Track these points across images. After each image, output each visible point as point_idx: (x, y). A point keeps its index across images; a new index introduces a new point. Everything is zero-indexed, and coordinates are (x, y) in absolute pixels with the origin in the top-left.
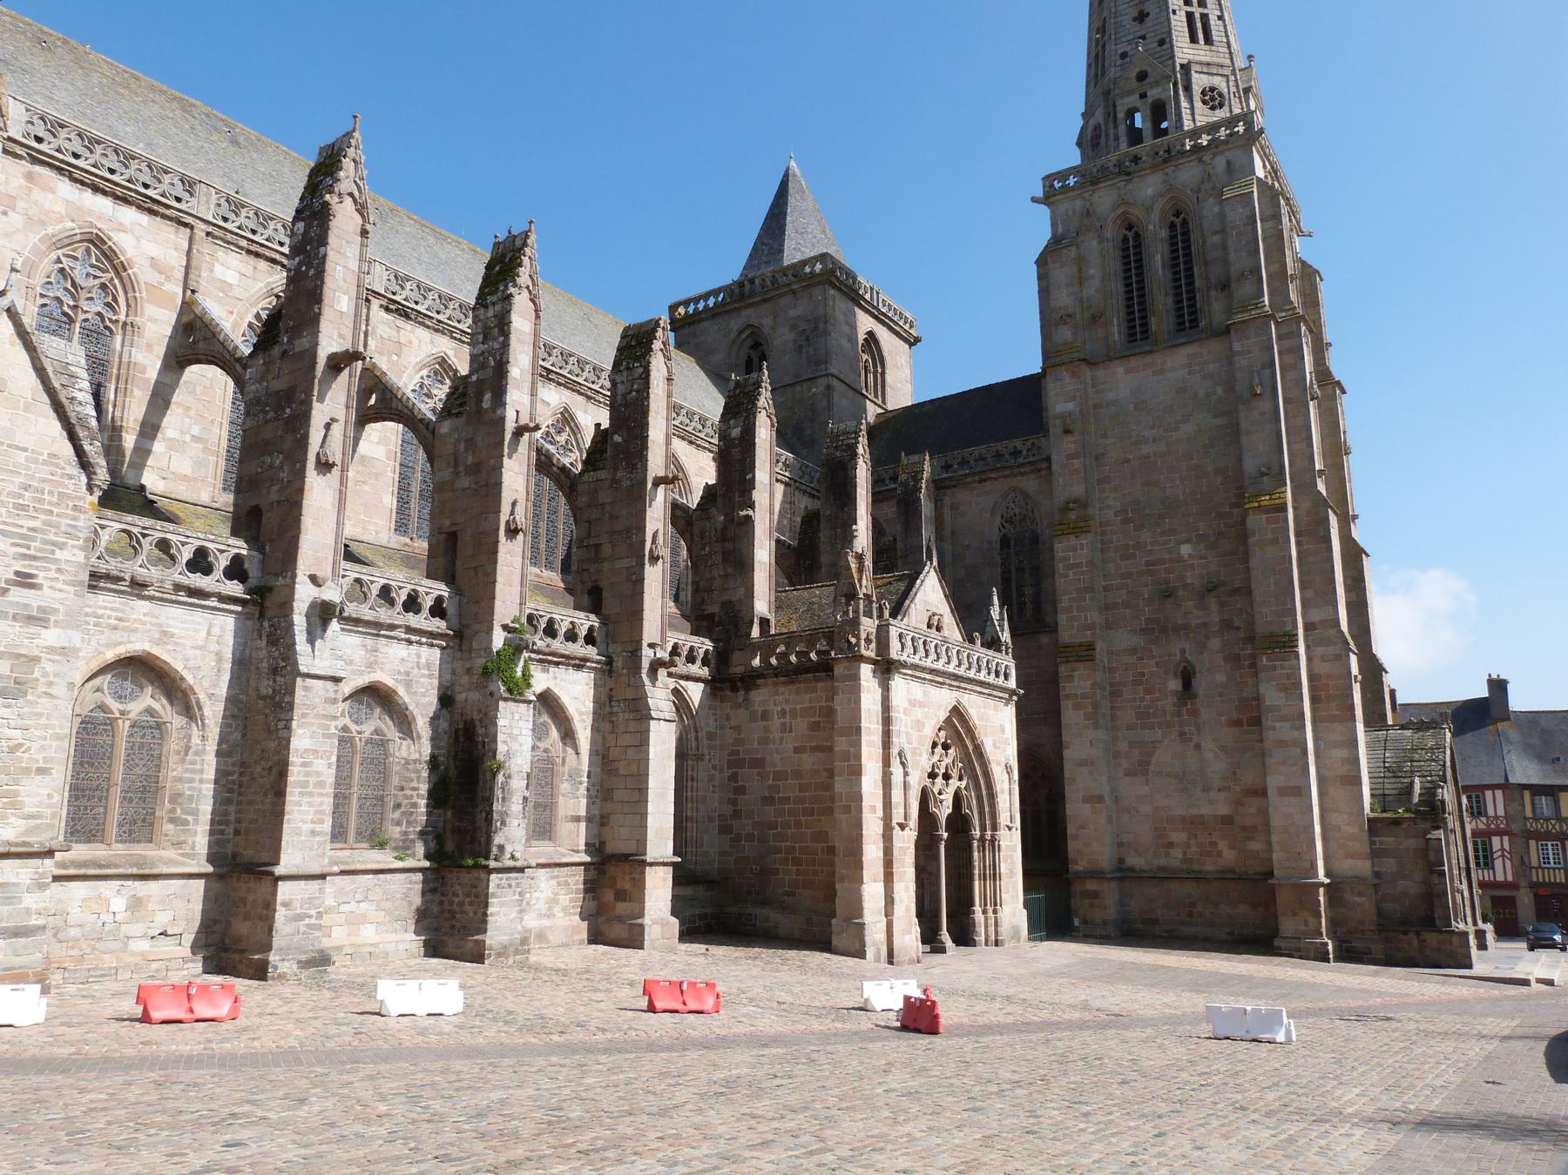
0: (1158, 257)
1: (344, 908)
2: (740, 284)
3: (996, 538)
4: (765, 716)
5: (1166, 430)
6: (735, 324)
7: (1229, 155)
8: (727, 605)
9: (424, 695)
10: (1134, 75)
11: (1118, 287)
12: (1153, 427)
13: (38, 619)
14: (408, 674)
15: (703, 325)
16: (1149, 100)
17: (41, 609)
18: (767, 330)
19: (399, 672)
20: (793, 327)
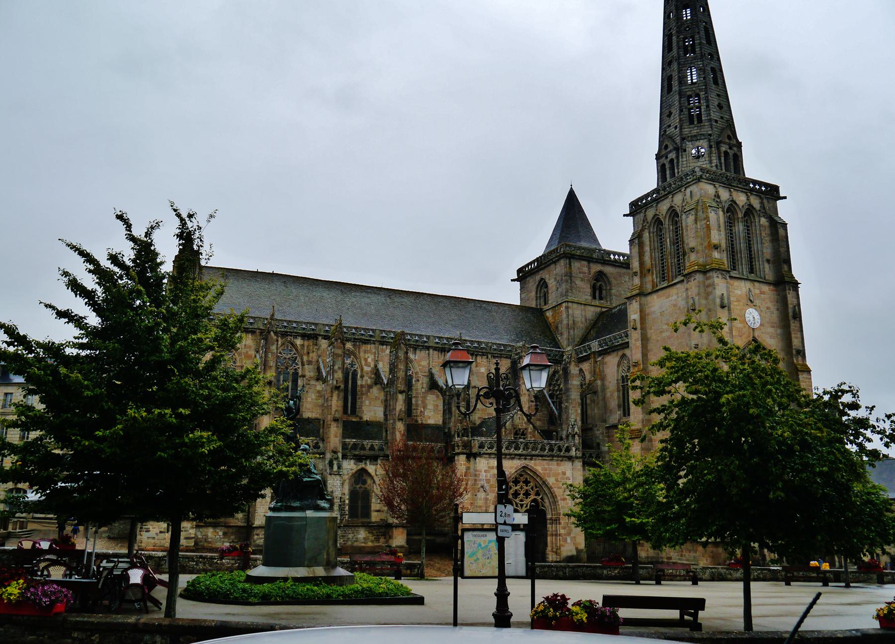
0: (668, 240)
3: (620, 378)
10: (663, 147)
11: (657, 255)
15: (528, 279)
16: (669, 159)
18: (547, 281)
20: (555, 279)
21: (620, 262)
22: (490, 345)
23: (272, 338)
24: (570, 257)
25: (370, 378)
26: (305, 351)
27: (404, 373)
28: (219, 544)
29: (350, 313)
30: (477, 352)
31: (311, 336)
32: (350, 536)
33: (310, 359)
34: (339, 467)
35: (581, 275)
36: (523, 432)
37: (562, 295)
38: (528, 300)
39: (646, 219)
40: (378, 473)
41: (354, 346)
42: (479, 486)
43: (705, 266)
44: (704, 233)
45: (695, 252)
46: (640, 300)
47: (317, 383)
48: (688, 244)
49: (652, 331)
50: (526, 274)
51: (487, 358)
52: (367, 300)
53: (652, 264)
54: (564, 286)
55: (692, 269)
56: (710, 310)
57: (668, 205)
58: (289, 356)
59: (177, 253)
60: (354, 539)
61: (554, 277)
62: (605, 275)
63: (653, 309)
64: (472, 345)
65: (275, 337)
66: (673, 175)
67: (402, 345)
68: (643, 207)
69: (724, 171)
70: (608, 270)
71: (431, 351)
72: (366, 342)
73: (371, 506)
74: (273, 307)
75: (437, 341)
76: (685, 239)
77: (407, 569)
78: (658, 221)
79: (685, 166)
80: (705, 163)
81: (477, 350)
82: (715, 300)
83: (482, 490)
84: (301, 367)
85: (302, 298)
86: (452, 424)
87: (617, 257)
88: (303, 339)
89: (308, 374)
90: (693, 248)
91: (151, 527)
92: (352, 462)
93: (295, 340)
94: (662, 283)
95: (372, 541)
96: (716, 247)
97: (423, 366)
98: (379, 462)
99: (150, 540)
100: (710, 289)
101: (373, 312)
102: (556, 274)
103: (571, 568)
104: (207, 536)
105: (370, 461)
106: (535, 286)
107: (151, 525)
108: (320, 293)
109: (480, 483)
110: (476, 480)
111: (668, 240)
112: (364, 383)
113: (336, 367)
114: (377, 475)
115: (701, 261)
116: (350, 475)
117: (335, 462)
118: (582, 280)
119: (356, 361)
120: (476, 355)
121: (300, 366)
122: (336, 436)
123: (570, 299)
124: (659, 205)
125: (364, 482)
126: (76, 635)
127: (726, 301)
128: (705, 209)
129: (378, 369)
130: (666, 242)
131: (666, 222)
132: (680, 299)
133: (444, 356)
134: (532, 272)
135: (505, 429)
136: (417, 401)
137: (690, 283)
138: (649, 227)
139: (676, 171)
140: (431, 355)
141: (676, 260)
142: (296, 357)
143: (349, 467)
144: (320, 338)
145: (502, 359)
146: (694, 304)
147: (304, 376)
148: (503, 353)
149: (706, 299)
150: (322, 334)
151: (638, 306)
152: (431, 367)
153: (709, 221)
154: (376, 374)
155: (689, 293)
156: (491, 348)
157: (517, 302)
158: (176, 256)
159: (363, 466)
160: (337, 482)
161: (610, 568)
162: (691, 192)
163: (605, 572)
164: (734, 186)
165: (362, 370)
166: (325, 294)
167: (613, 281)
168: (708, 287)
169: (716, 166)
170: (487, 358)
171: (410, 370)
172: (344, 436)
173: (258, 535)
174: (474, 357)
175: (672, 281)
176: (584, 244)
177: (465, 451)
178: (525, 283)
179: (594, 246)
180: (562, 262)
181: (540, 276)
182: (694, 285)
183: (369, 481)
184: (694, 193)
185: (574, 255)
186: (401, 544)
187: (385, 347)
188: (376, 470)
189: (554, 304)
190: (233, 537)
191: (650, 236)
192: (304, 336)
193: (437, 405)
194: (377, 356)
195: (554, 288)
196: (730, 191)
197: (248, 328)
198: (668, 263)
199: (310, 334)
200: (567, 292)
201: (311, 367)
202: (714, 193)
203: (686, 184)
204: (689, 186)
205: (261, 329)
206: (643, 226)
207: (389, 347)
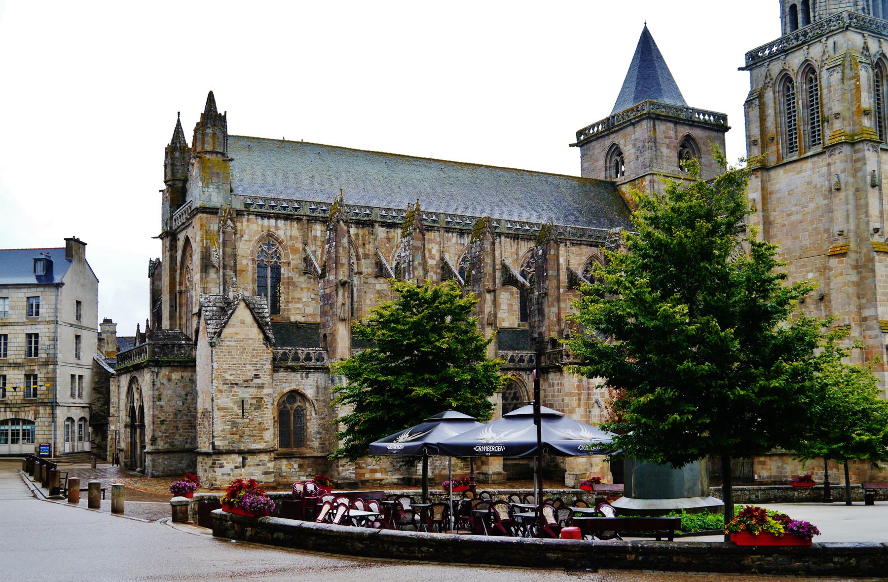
0: (800, 102)
1: (369, 467)
2: (608, 119)
4: (553, 386)
5: (802, 207)
6: (608, 142)
7: (835, 38)
8: (540, 334)
11: (784, 120)
12: (796, 205)
13: (261, 387)
15: (593, 143)
17: (262, 384)
18: (621, 147)
20: (634, 145)
21: (711, 124)
23: (342, 229)
24: (656, 118)
25: (436, 273)
26: (360, 241)
27: (491, 269)
28: (295, 478)
29: (403, 193)
31: (366, 223)
32: (438, 463)
33: (367, 252)
35: (667, 141)
37: (644, 166)
38: (594, 170)
39: (770, 75)
42: (594, 401)
43: (852, 136)
44: (852, 95)
45: (841, 119)
46: (762, 175)
47: (376, 281)
48: (830, 109)
49: (776, 213)
50: (591, 137)
51: (566, 245)
53: (777, 132)
54: (647, 155)
55: (837, 139)
56: (857, 190)
57: (802, 59)
59: (199, 120)
60: (442, 467)
61: (633, 142)
62: (693, 140)
63: (777, 187)
64: (531, 228)
65: (345, 228)
66: (807, 21)
68: (765, 60)
69: (872, 15)
70: (697, 133)
71: (503, 238)
75: (509, 226)
76: (825, 101)
78: (786, 78)
79: (824, 8)
80: (848, 5)
82: (865, 177)
83: (596, 405)
84: (356, 262)
85: (344, 174)
86: (544, 328)
87: (707, 117)
88: (357, 227)
89: (365, 270)
90: (839, 114)
91: (225, 462)
94: (790, 155)
95: (461, 468)
96: (866, 113)
99: (226, 477)
100: (859, 165)
102: (636, 140)
103: (763, 490)
106: (604, 153)
107: (225, 460)
108: (362, 166)
109: (594, 398)
110: (589, 394)
111: (800, 102)
113: (416, 263)
115: (848, 130)
118: (668, 147)
123: (654, 170)
124: (788, 58)
126: (836, 559)
127: (877, 181)
128: (854, 65)
129: (446, 262)
130: (798, 104)
131: (798, 81)
132: (816, 175)
133: (518, 244)
134: (598, 136)
137: (833, 157)
138: (774, 85)
139: (812, 14)
140: (503, 244)
141: (809, 126)
144: (377, 225)
145: (582, 246)
146: (838, 183)
147: (360, 273)
148: (584, 239)
149: (855, 176)
150: (379, 220)
151: (760, 183)
152: (503, 258)
153: (858, 80)
154: (443, 268)
155: (833, 169)
157: (578, 174)
158: (198, 124)
162: (835, 43)
163: (796, 493)
164: (885, 35)
167: (703, 148)
168: (855, 161)
169: (863, 9)
170: (566, 245)
173: (343, 466)
175: (805, 152)
176: (667, 101)
177: (576, 361)
178: (589, 149)
179: (679, 104)
180: (645, 124)
181: (611, 140)
182: (839, 161)
184: (838, 45)
185: (658, 115)
187: (450, 234)
189: (633, 177)
190: (309, 470)
191: (775, 98)
192: (359, 223)
193: (512, 305)
194: (442, 246)
195: (633, 157)
196: (879, 41)
197: (293, 215)
198: (800, 130)
199: (366, 221)
200: (651, 162)
201: (368, 261)
202: (862, 45)
203: (828, 33)
204: (832, 36)
206: (765, 84)
207: (455, 235)
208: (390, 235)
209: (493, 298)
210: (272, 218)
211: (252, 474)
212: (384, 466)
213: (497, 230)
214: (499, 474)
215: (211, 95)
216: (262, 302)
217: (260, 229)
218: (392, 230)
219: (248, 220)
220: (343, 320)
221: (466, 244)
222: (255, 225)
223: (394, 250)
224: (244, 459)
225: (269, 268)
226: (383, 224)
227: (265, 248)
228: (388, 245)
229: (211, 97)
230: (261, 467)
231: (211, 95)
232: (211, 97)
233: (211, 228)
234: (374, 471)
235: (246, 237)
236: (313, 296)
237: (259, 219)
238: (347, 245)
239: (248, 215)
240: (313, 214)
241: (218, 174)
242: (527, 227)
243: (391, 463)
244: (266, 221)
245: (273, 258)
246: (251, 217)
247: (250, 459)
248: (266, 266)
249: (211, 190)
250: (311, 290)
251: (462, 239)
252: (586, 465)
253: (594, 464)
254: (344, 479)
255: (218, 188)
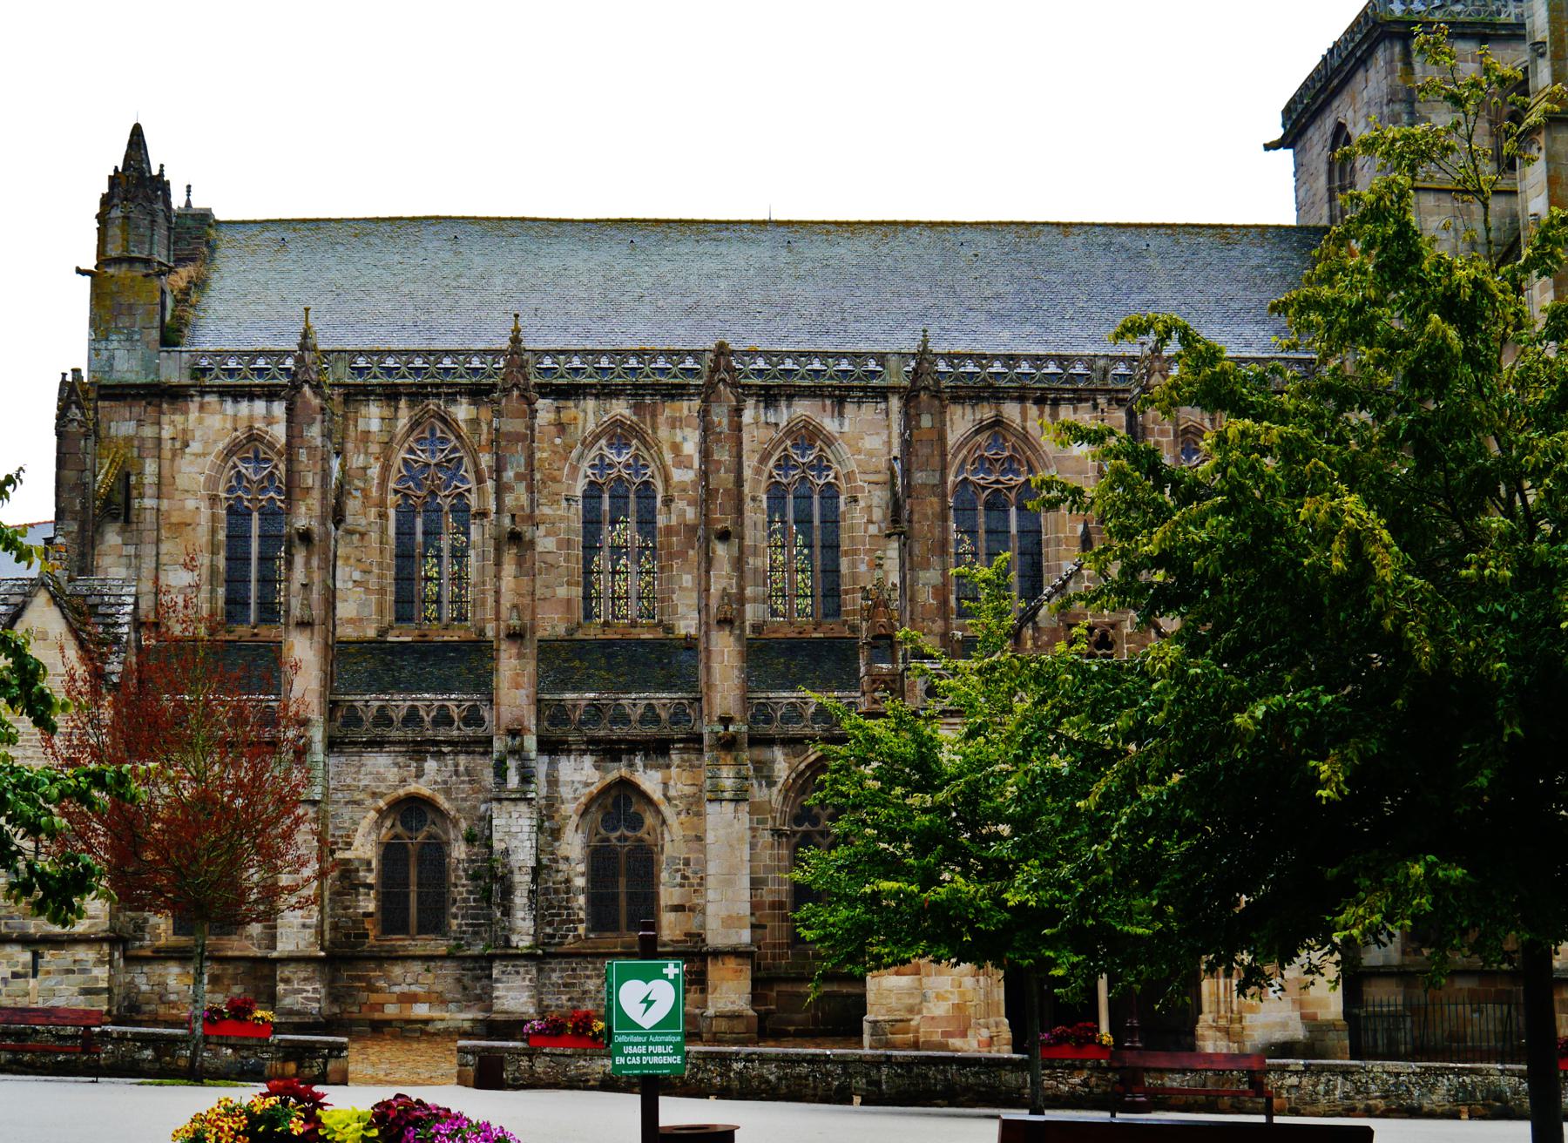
1: (397, 989)
9: (464, 800)
14: (445, 782)
19: (436, 782)
22: (1101, 363)
23: (307, 404)
30: (1058, 390)
34: (526, 778)
36: (1104, 635)
40: (672, 793)
41: (637, 408)
51: (1095, 407)
52: (711, 265)
58: (440, 457)
67: (721, 386)
72: (675, 392)
73: (658, 893)
74: (307, 310)
77: (286, 1060)
81: (1055, 385)
84: (474, 489)
88: (474, 403)
92: (588, 760)
93: (452, 409)
97: (870, 453)
98: (675, 758)
101: (724, 297)
103: (900, 1065)
104: (164, 985)
105: (646, 756)
112: (674, 522)
113: (509, 475)
114: (669, 799)
116: (583, 800)
117: (512, 764)
119: (647, 456)
120: (1056, 403)
121: (473, 485)
122: (518, 686)
125: (636, 822)
135: (1036, 628)
136: (854, 565)
142: (461, 458)
143: (577, 777)
156: (1106, 372)
157: (1289, 218)
159: (624, 772)
160: (521, 822)
161: (1054, 1068)
165: (667, 480)
166: (573, 262)
170: (1095, 407)
171: (829, 468)
172: (541, 682)
173: (287, 981)
174: (1047, 409)
178: (1303, 149)
180: (1381, 57)
183: (649, 819)
186: (736, 1008)
188: (666, 785)
205: (348, 386)
208: (565, 416)
209: (735, 553)
210: (259, 397)
211: (52, 992)
212: (439, 988)
213: (875, 382)
214: (734, 1016)
215: (137, 132)
216: (125, 590)
217: (229, 425)
218: (571, 404)
219: (202, 407)
220: (304, 624)
221: (783, 424)
222: (218, 417)
223: (574, 454)
224: (36, 956)
225: (255, 515)
226: (547, 391)
227: (247, 470)
228: (558, 441)
229: (137, 138)
230: (77, 978)
231: (137, 132)
232: (137, 138)
233: (113, 431)
234: (410, 999)
235: (195, 447)
236: (357, 576)
237: (229, 406)
238: (318, 442)
239: (202, 394)
240: (359, 381)
241: (130, 307)
242: (970, 368)
243: (459, 980)
244: (244, 407)
245: (263, 490)
246: (207, 399)
247: (49, 957)
248: (248, 513)
249: (115, 344)
250: (352, 561)
251: (771, 412)
252: (911, 995)
253: (931, 994)
254: (291, 1012)
255: (129, 339)
